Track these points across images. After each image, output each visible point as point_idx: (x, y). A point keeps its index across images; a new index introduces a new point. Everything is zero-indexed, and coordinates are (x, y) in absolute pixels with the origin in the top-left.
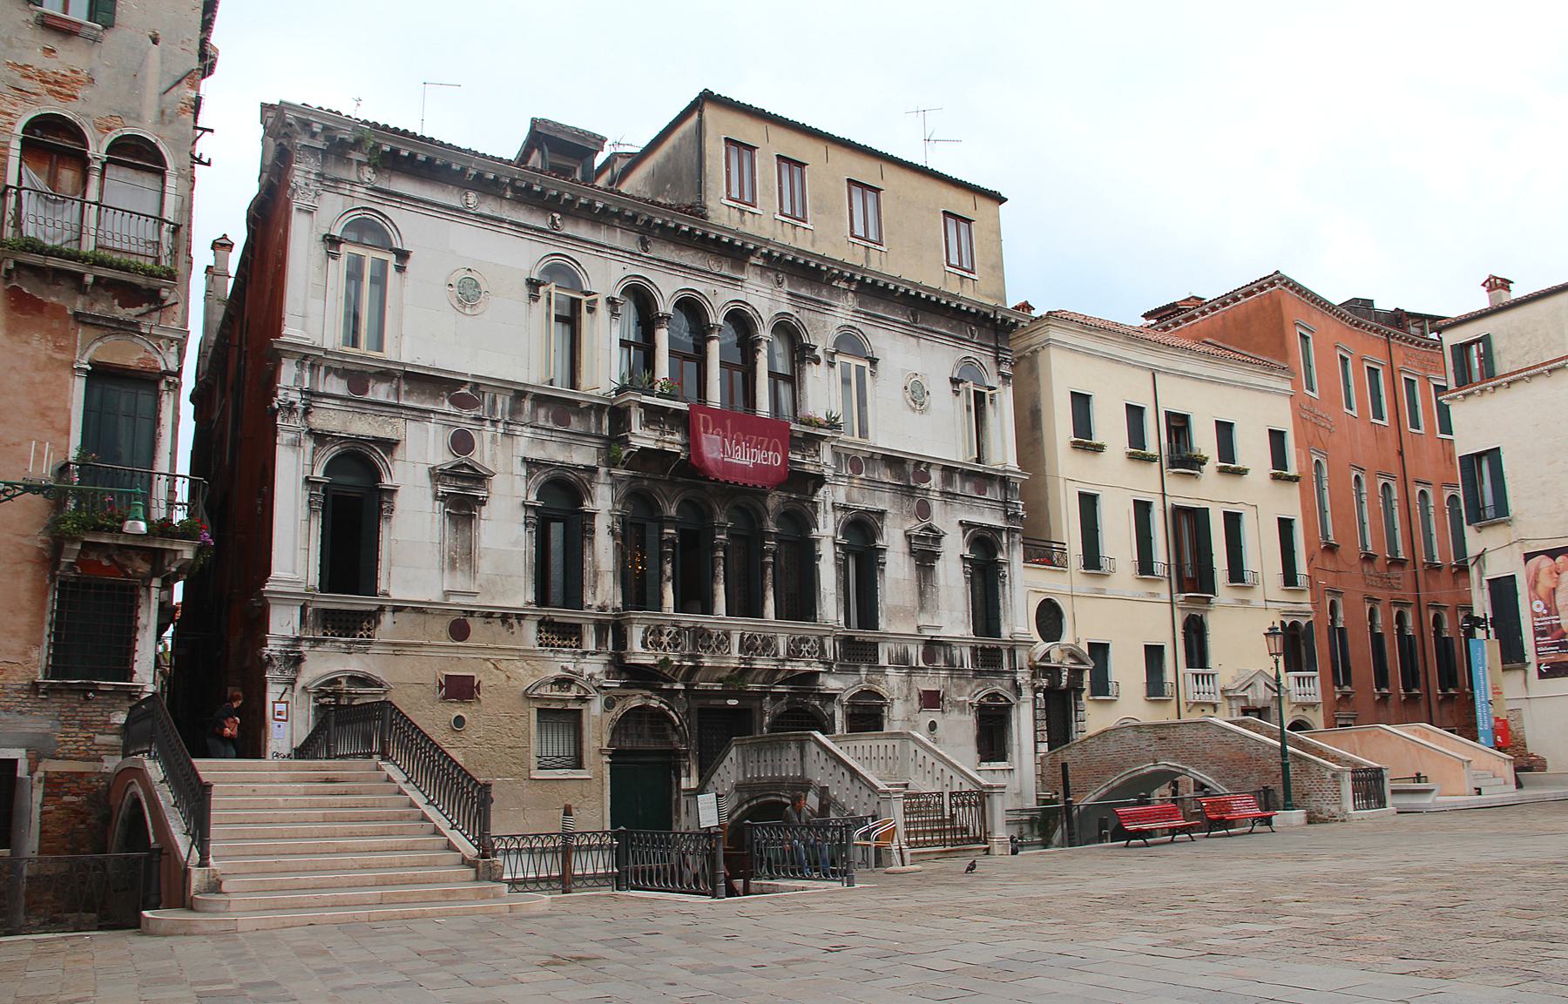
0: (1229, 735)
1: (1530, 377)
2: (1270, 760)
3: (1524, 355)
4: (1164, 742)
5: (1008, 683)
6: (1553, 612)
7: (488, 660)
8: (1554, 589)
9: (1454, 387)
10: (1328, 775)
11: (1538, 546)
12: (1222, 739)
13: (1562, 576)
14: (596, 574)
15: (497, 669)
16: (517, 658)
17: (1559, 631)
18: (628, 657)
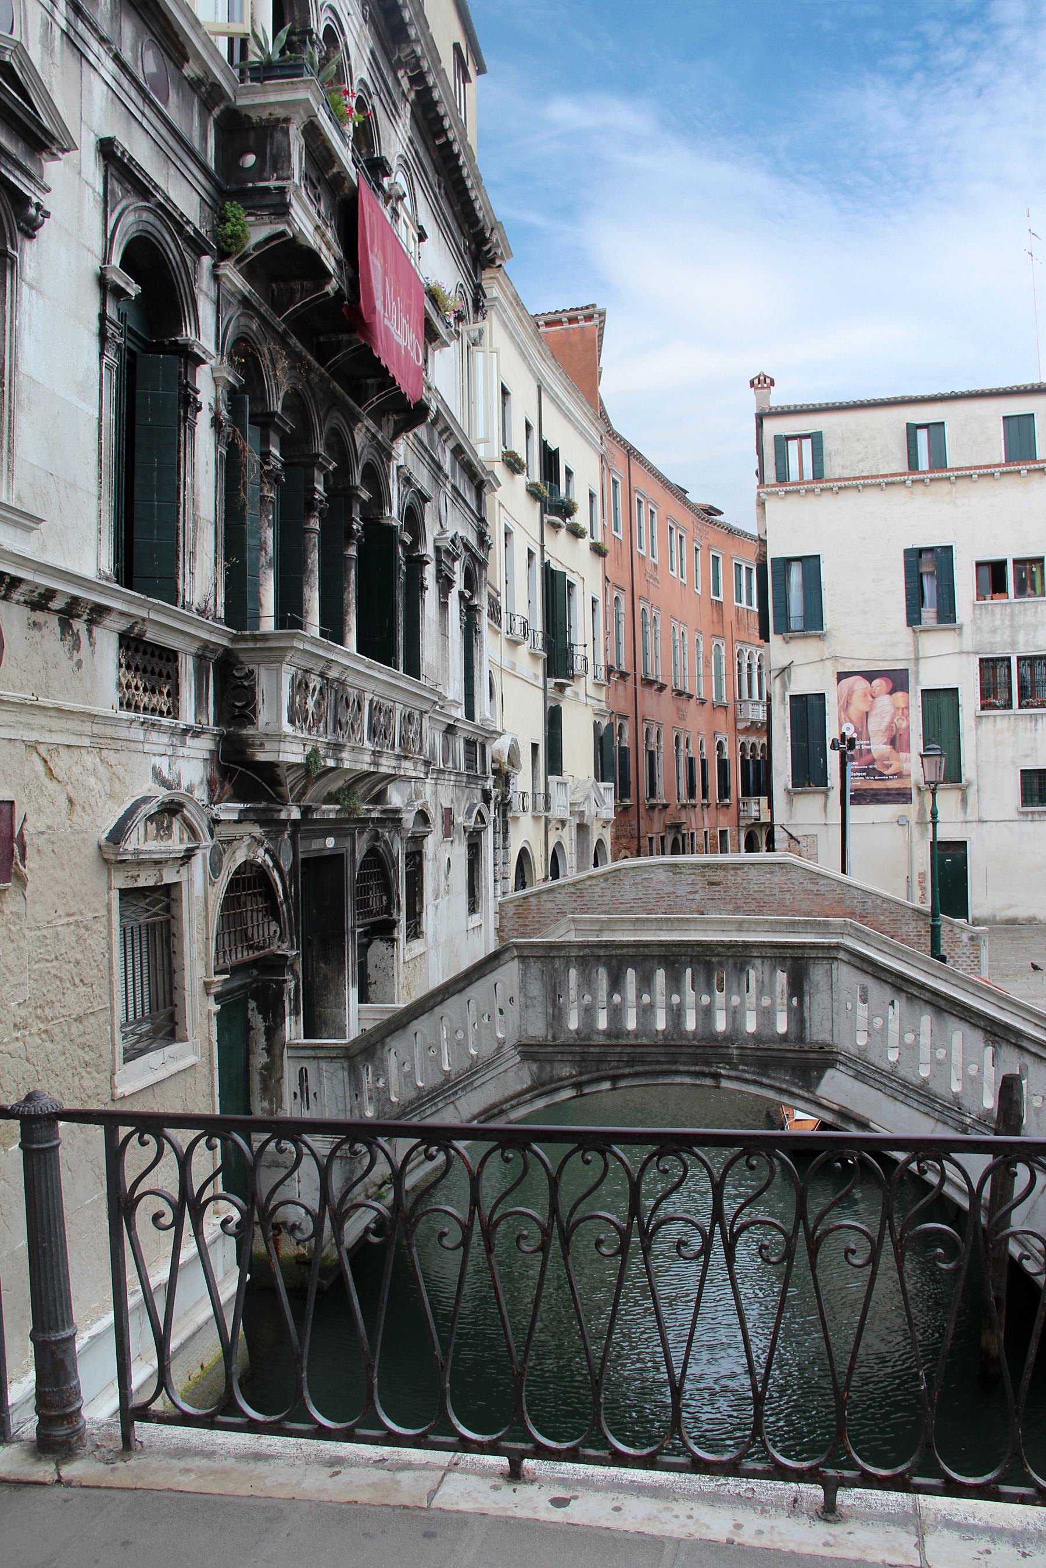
0: (822, 882)
1: (864, 486)
2: (882, 917)
3: (859, 462)
4: (718, 888)
5: (479, 793)
6: (864, 736)
7: (33, 747)
8: (867, 713)
9: (773, 481)
10: (965, 937)
11: (853, 666)
12: (810, 887)
13: (877, 700)
14: (195, 523)
15: (50, 773)
16: (86, 742)
17: (868, 758)
18: (268, 746)
